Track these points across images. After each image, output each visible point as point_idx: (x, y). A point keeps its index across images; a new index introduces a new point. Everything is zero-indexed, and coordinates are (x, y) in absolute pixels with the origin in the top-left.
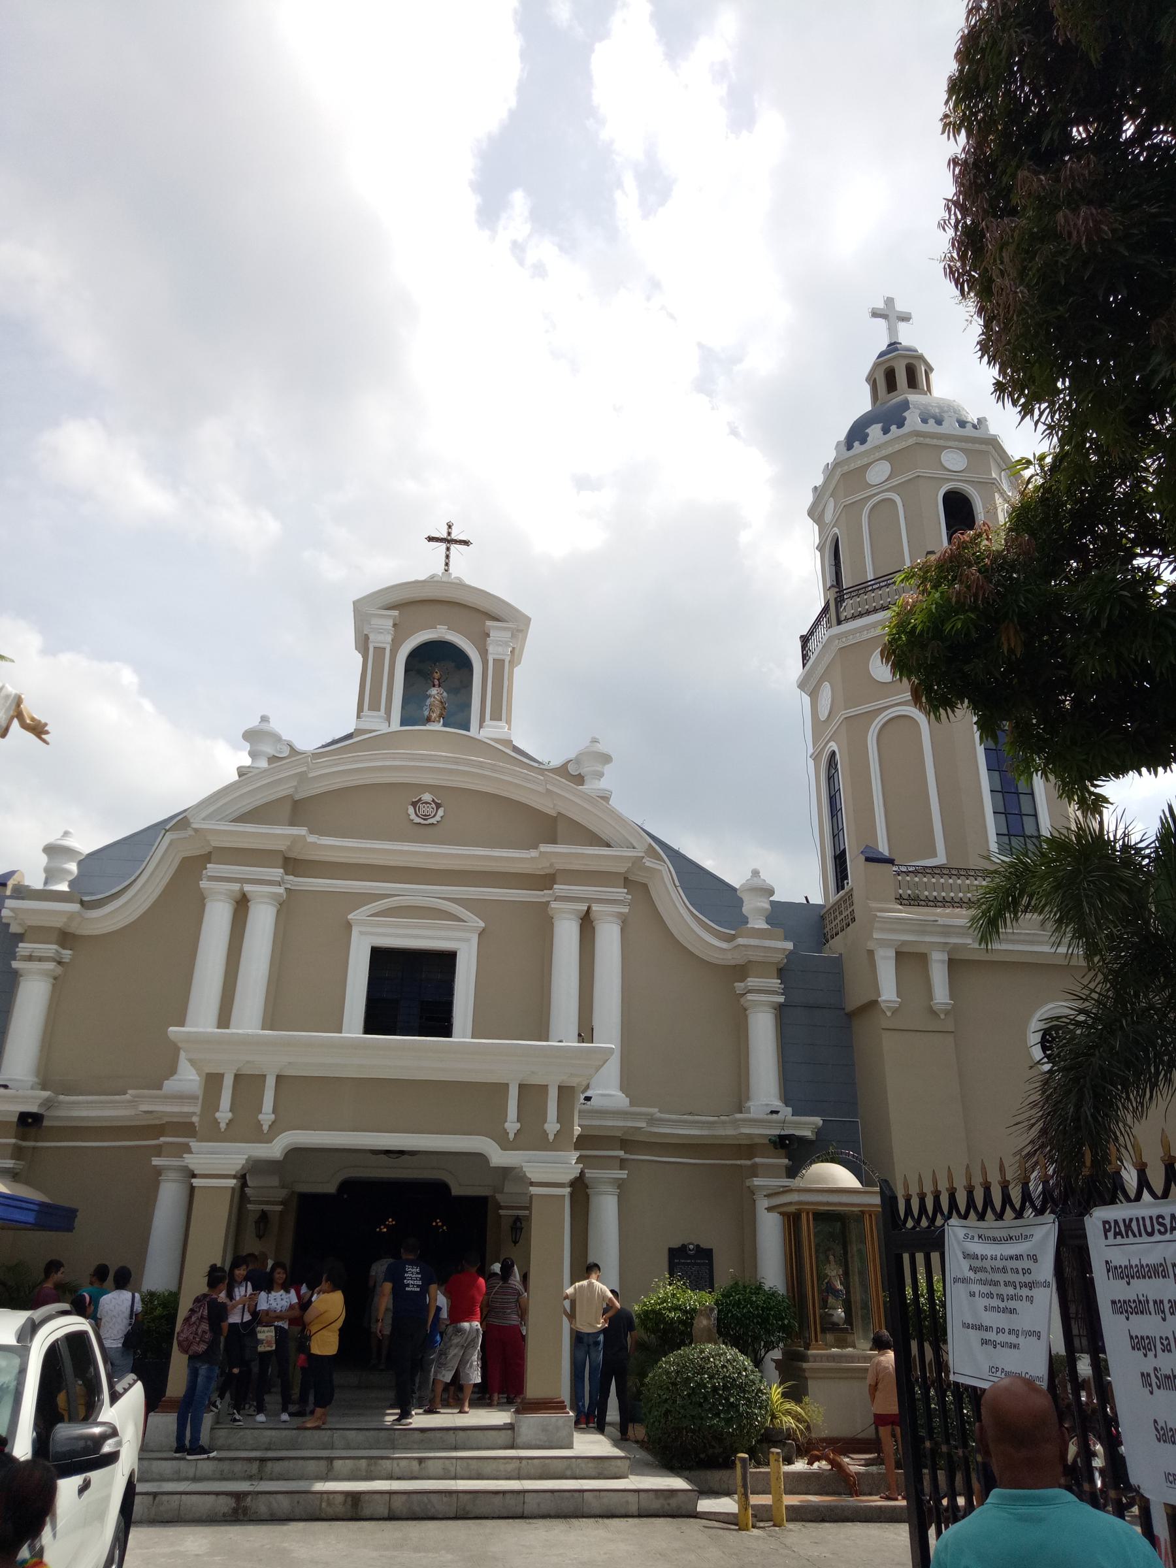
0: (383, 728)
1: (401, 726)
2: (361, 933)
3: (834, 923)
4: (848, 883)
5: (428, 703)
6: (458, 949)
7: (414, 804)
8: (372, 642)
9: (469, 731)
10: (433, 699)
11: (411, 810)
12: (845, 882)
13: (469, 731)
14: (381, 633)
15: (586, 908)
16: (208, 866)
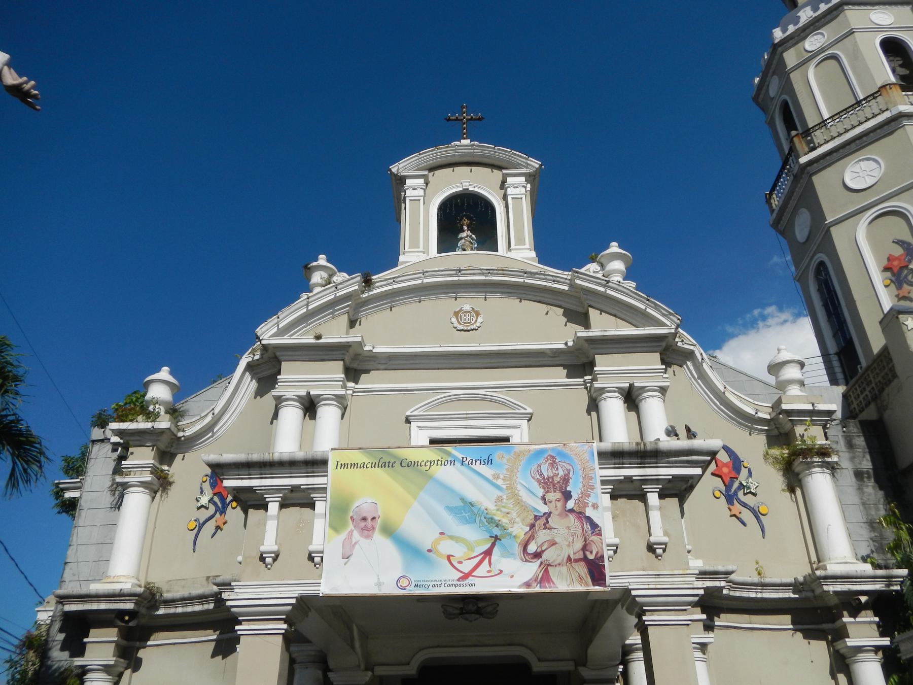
0: (423, 257)
1: (438, 253)
2: (420, 428)
3: (861, 398)
4: (861, 368)
5: (459, 244)
6: (511, 436)
7: (456, 314)
8: (408, 197)
9: (498, 252)
10: (463, 241)
11: (454, 320)
12: (859, 366)
13: (497, 251)
14: (416, 189)
15: (628, 385)
16: (278, 377)
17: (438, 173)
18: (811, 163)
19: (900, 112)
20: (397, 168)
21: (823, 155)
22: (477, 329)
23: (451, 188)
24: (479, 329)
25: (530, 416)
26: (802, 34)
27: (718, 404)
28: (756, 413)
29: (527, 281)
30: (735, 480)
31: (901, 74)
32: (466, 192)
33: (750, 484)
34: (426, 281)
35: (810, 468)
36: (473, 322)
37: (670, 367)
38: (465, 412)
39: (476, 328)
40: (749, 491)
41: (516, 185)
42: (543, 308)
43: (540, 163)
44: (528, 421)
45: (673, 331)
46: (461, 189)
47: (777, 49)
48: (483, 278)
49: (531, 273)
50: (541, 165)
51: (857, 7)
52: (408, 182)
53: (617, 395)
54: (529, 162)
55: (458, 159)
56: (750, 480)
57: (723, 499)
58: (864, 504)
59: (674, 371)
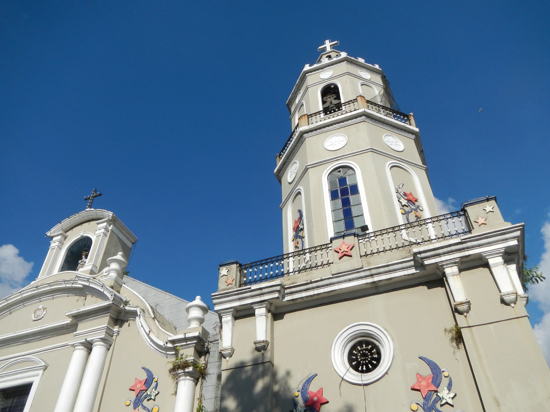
10: (79, 265)
11: (33, 315)
14: (55, 242)
17: (74, 229)
18: (279, 171)
19: (301, 132)
20: (50, 233)
21: (282, 165)
22: (42, 319)
23: (75, 237)
24: (43, 318)
25: (43, 367)
26: (296, 95)
27: (149, 341)
28: (164, 345)
29: (67, 286)
30: (144, 391)
31: (335, 103)
32: (82, 238)
33: (153, 393)
34: (23, 296)
35: (179, 378)
36: (41, 314)
37: (127, 322)
38: (15, 370)
39: (41, 318)
40: (150, 398)
41: (100, 228)
42: (77, 297)
43: (112, 213)
44: (44, 370)
45: (111, 302)
46: (80, 237)
47: (289, 106)
48: (49, 288)
49: (67, 281)
50: (113, 214)
51: (313, 73)
52: (54, 239)
53: (82, 347)
54: (109, 214)
55: (82, 220)
56: (154, 390)
57: (132, 405)
58: (216, 397)
59: (129, 324)
